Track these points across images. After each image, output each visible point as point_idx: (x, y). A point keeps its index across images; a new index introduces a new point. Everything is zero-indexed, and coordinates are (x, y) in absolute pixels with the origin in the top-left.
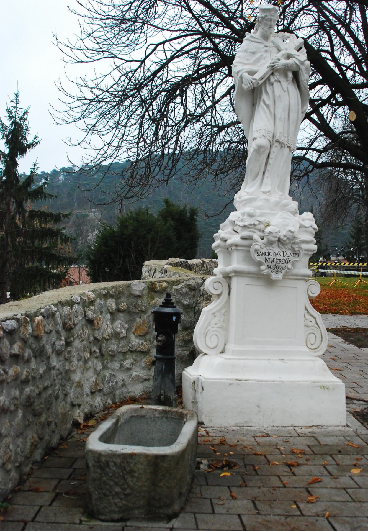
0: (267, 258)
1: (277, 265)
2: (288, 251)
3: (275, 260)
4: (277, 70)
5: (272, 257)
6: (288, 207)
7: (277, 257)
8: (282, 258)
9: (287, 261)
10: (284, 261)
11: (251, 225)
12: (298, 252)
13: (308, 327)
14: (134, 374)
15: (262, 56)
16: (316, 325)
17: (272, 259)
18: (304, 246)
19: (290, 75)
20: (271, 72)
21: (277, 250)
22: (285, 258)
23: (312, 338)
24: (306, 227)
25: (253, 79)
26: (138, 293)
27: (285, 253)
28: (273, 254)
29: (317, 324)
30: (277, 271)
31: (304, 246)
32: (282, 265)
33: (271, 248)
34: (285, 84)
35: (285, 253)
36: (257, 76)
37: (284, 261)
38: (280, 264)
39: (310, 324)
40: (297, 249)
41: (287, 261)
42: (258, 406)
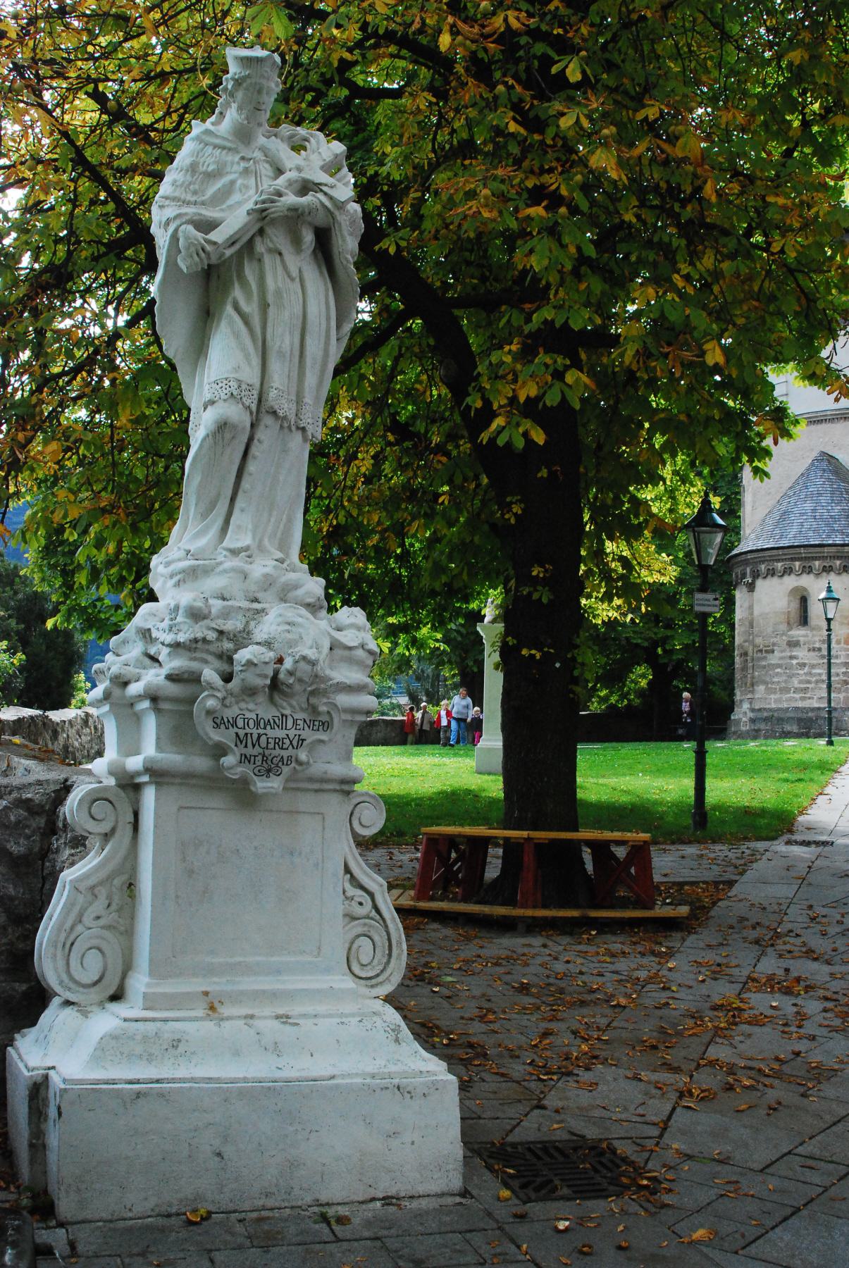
0: (241, 733)
1: (267, 752)
3: (263, 739)
4: (273, 222)
5: (255, 732)
6: (300, 592)
7: (268, 730)
9: (295, 743)
10: (287, 741)
11: (196, 640)
12: (324, 718)
13: (354, 919)
15: (233, 183)
16: (374, 913)
18: (343, 700)
19: (309, 237)
21: (268, 713)
22: (292, 733)
24: (350, 648)
25: (206, 240)
28: (257, 724)
30: (269, 771)
31: (343, 700)
34: (293, 262)
36: (218, 236)
37: (287, 741)
38: (278, 752)
40: (323, 708)
41: (295, 743)
42: (219, 1154)
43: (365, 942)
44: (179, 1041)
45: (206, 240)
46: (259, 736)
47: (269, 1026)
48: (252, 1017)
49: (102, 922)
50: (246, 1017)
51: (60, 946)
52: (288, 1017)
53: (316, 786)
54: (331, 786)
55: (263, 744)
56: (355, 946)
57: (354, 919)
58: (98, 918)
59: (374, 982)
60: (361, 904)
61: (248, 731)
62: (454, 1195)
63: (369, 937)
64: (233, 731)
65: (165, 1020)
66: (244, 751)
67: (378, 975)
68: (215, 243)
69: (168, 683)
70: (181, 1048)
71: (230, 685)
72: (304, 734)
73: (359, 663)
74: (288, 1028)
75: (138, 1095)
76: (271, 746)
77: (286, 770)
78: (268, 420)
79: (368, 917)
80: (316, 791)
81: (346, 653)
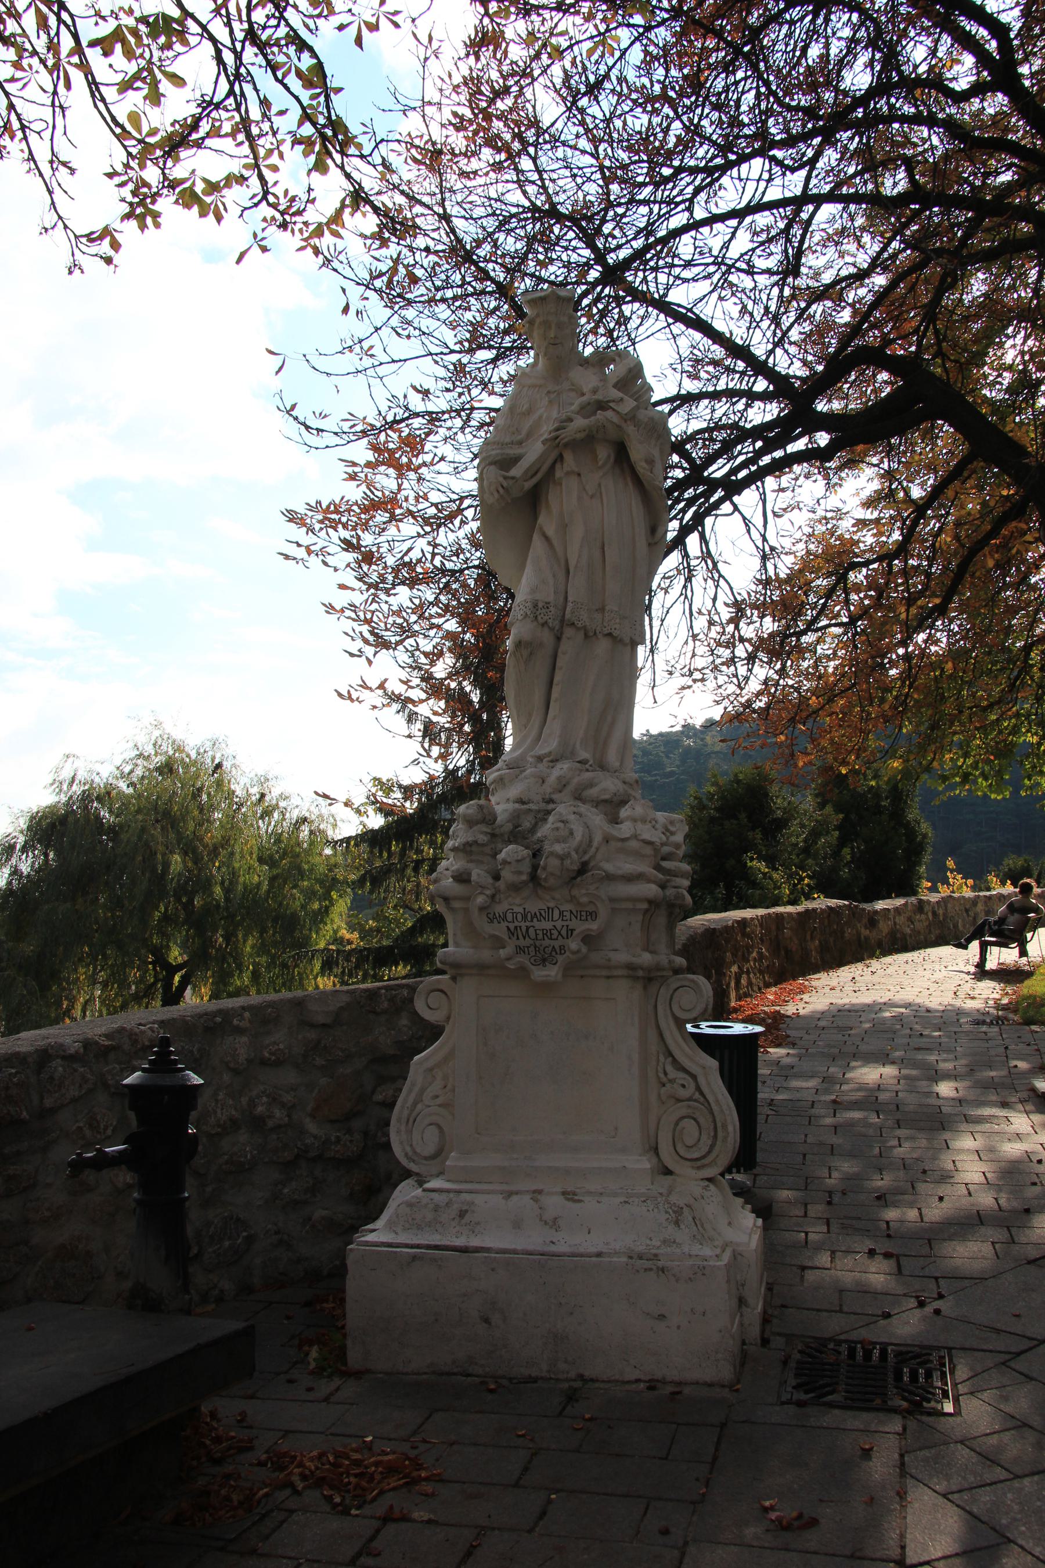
0: (512, 926)
1: (538, 943)
2: (567, 907)
3: (531, 930)
6: (593, 792)
8: (547, 925)
9: (564, 932)
12: (591, 908)
13: (679, 1100)
14: (319, 1214)
15: (540, 417)
16: (697, 1095)
17: (524, 929)
19: (604, 453)
20: (554, 455)
21: (534, 906)
24: (623, 840)
25: (505, 478)
26: (321, 1019)
27: (556, 913)
28: (525, 917)
29: (702, 1093)
30: (544, 960)
33: (518, 901)
35: (556, 913)
37: (555, 932)
38: (547, 942)
39: (683, 1093)
40: (584, 900)
41: (564, 932)
43: (689, 1125)
44: (466, 1211)
45: (505, 478)
46: (528, 928)
47: (554, 1203)
48: (540, 1192)
49: (439, 1101)
50: (534, 1192)
52: (574, 1194)
53: (604, 973)
54: (620, 972)
55: (533, 935)
56: (679, 1128)
57: (679, 1100)
58: (437, 1097)
59: (699, 1163)
60: (683, 1086)
61: (516, 924)
62: (723, 1386)
63: (695, 1119)
64: (504, 924)
65: (459, 1192)
66: (518, 943)
67: (704, 1157)
68: (513, 478)
69: (455, 885)
70: (467, 1218)
71: (497, 884)
72: (574, 923)
73: (637, 854)
74: (570, 1204)
75: (414, 1258)
76: (540, 936)
77: (560, 959)
78: (569, 632)
79: (690, 1099)
80: (608, 977)
81: (619, 844)
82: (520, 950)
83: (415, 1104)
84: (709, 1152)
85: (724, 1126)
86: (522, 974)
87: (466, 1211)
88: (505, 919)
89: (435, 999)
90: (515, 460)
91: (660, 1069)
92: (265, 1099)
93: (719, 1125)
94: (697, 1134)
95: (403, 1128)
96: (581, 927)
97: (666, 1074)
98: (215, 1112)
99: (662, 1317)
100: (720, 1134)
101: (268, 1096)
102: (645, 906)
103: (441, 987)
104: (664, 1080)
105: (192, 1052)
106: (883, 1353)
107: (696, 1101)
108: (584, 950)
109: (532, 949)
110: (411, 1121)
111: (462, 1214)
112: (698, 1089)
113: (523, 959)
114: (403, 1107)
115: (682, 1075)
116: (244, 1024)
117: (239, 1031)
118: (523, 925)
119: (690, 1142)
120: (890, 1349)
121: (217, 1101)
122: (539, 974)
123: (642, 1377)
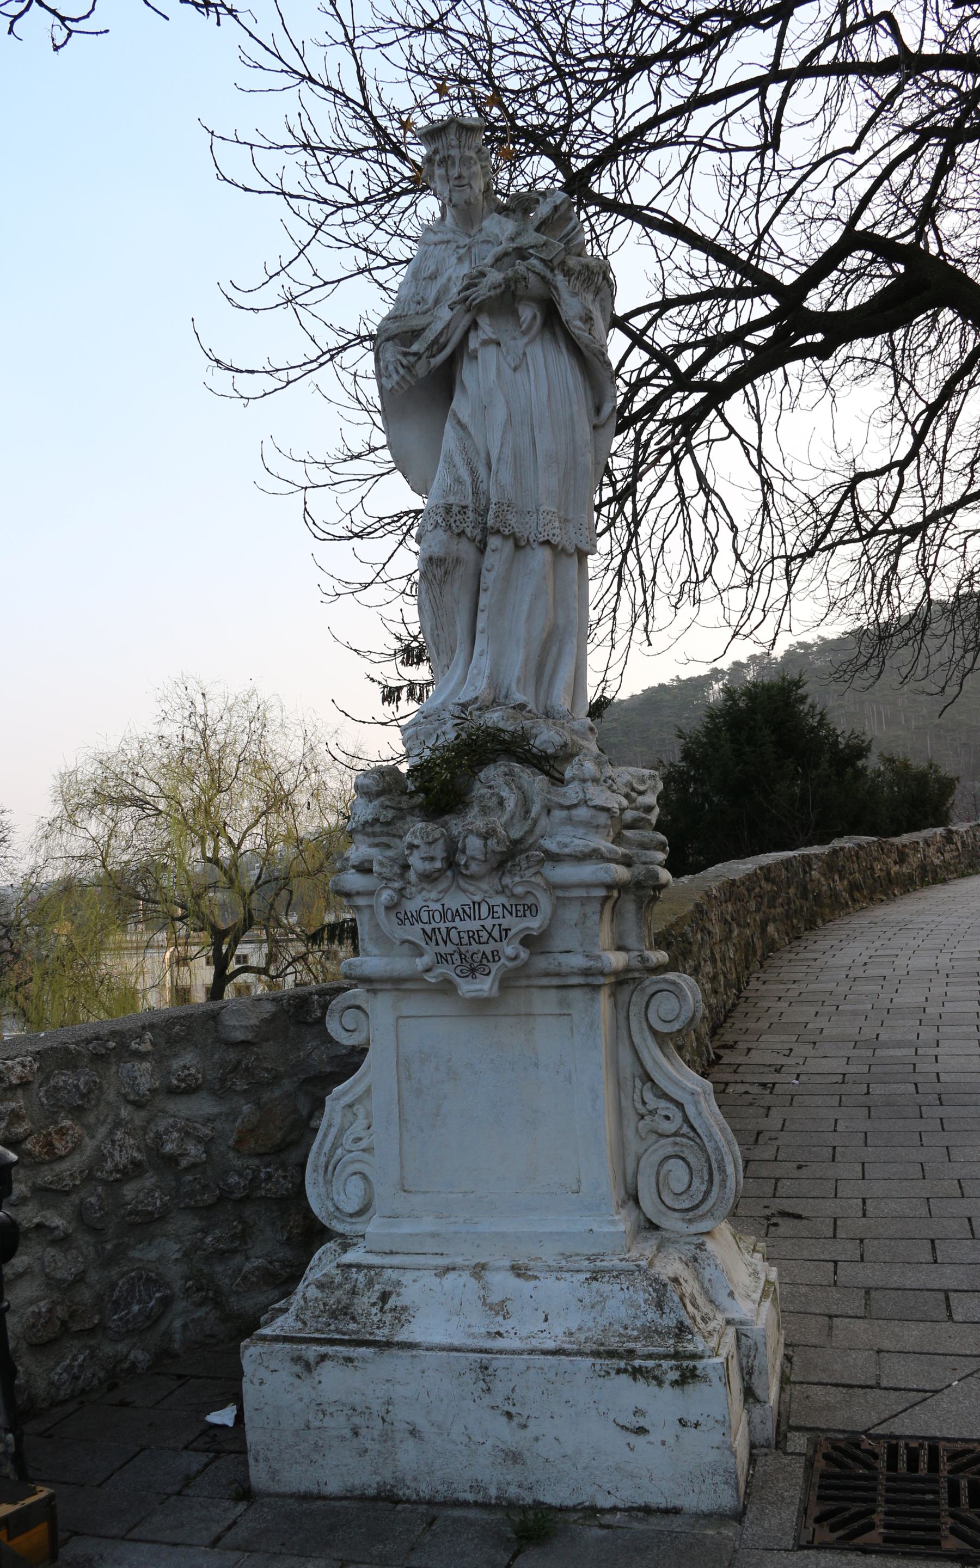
0: (428, 928)
1: (463, 949)
2: (500, 900)
3: (453, 933)
8: (474, 925)
9: (496, 934)
10: (484, 935)
12: (530, 900)
13: (662, 1136)
16: (685, 1129)
17: (444, 931)
19: (527, 313)
20: (465, 321)
21: (455, 901)
22: (489, 923)
23: (678, 1171)
24: (569, 808)
26: (239, 1036)
27: (484, 909)
28: (443, 916)
30: (473, 971)
32: (482, 948)
33: (433, 895)
35: (484, 909)
37: (484, 935)
38: (475, 947)
39: (669, 1127)
41: (496, 934)
43: (676, 1166)
45: (405, 354)
46: (448, 930)
48: (483, 1267)
51: (321, 1171)
53: (556, 981)
56: (663, 1172)
57: (662, 1136)
60: (667, 1118)
61: (434, 925)
63: (683, 1159)
66: (437, 949)
70: (391, 1303)
77: (494, 967)
79: (675, 1134)
81: (564, 813)
82: (442, 958)
83: (334, 1148)
84: (702, 1202)
85: (722, 1170)
86: (447, 988)
87: (390, 1293)
88: (419, 919)
89: (350, 1019)
90: (416, 334)
91: (637, 1097)
92: (176, 1135)
93: (714, 1165)
94: (686, 1179)
95: (321, 1179)
96: (517, 925)
97: (644, 1103)
98: (112, 1155)
99: (641, 1431)
100: (717, 1178)
101: (179, 1131)
102: (602, 893)
103: (358, 1003)
104: (643, 1110)
105: (77, 1086)
106: (934, 1452)
107: (683, 1135)
108: (524, 954)
109: (456, 956)
110: (330, 1169)
111: (385, 1297)
112: (686, 1119)
113: (444, 970)
114: (319, 1154)
115: (663, 1104)
116: (146, 1047)
117: (141, 1056)
118: (443, 926)
119: (679, 1188)
120: (942, 1445)
121: (113, 1142)
122: (468, 988)
123: (621, 1505)
